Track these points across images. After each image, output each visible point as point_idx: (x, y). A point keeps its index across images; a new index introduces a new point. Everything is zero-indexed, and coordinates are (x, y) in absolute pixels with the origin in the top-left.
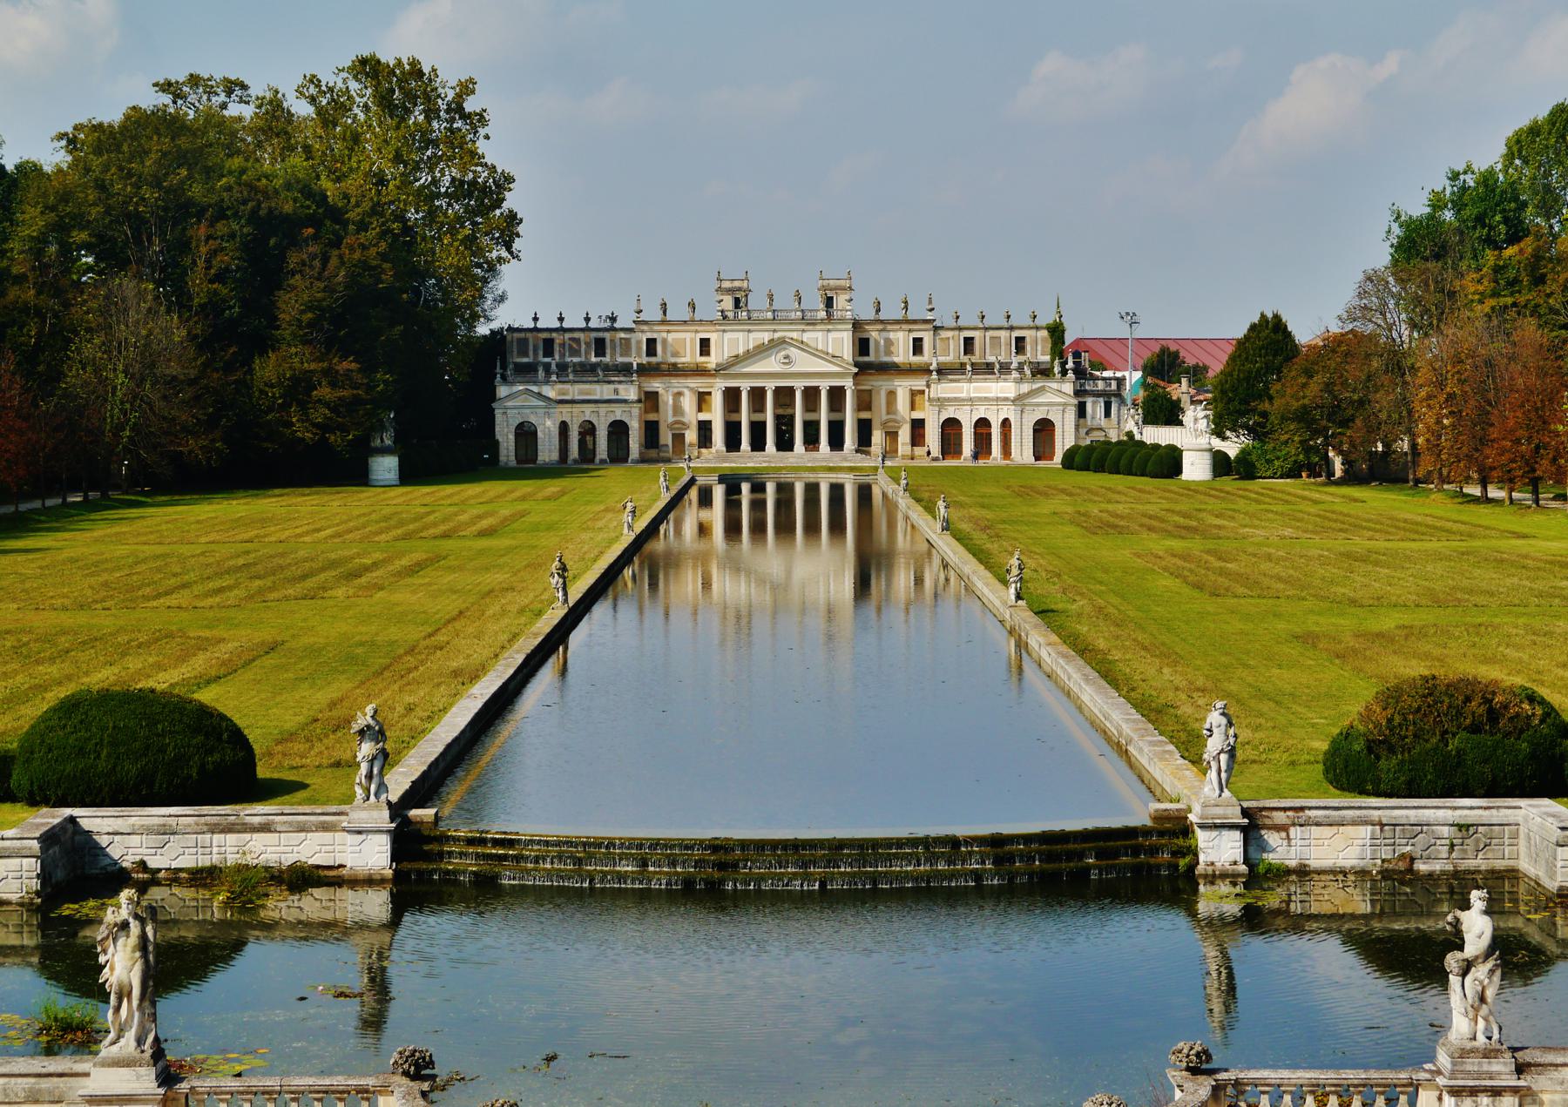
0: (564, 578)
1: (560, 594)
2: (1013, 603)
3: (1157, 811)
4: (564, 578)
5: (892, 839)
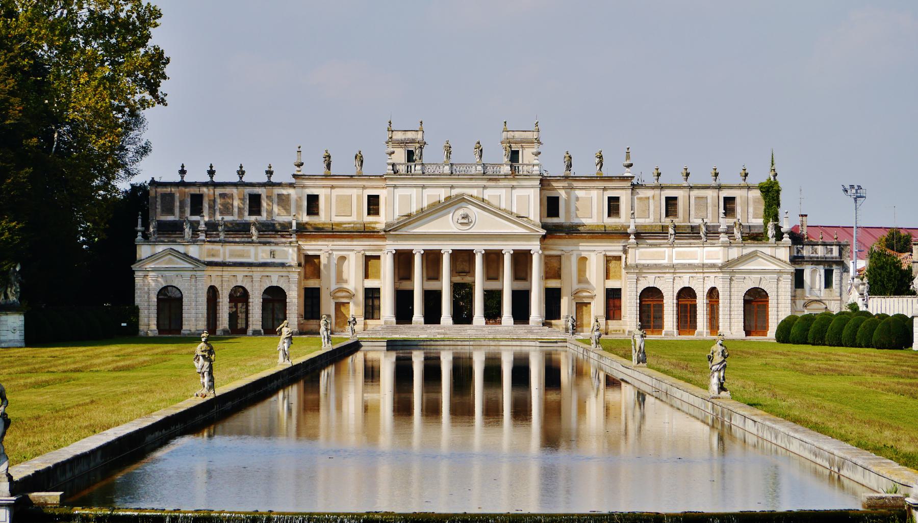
0: (210, 361)
1: (206, 379)
2: (716, 394)
3: (870, 499)
4: (210, 361)
5: (573, 515)
